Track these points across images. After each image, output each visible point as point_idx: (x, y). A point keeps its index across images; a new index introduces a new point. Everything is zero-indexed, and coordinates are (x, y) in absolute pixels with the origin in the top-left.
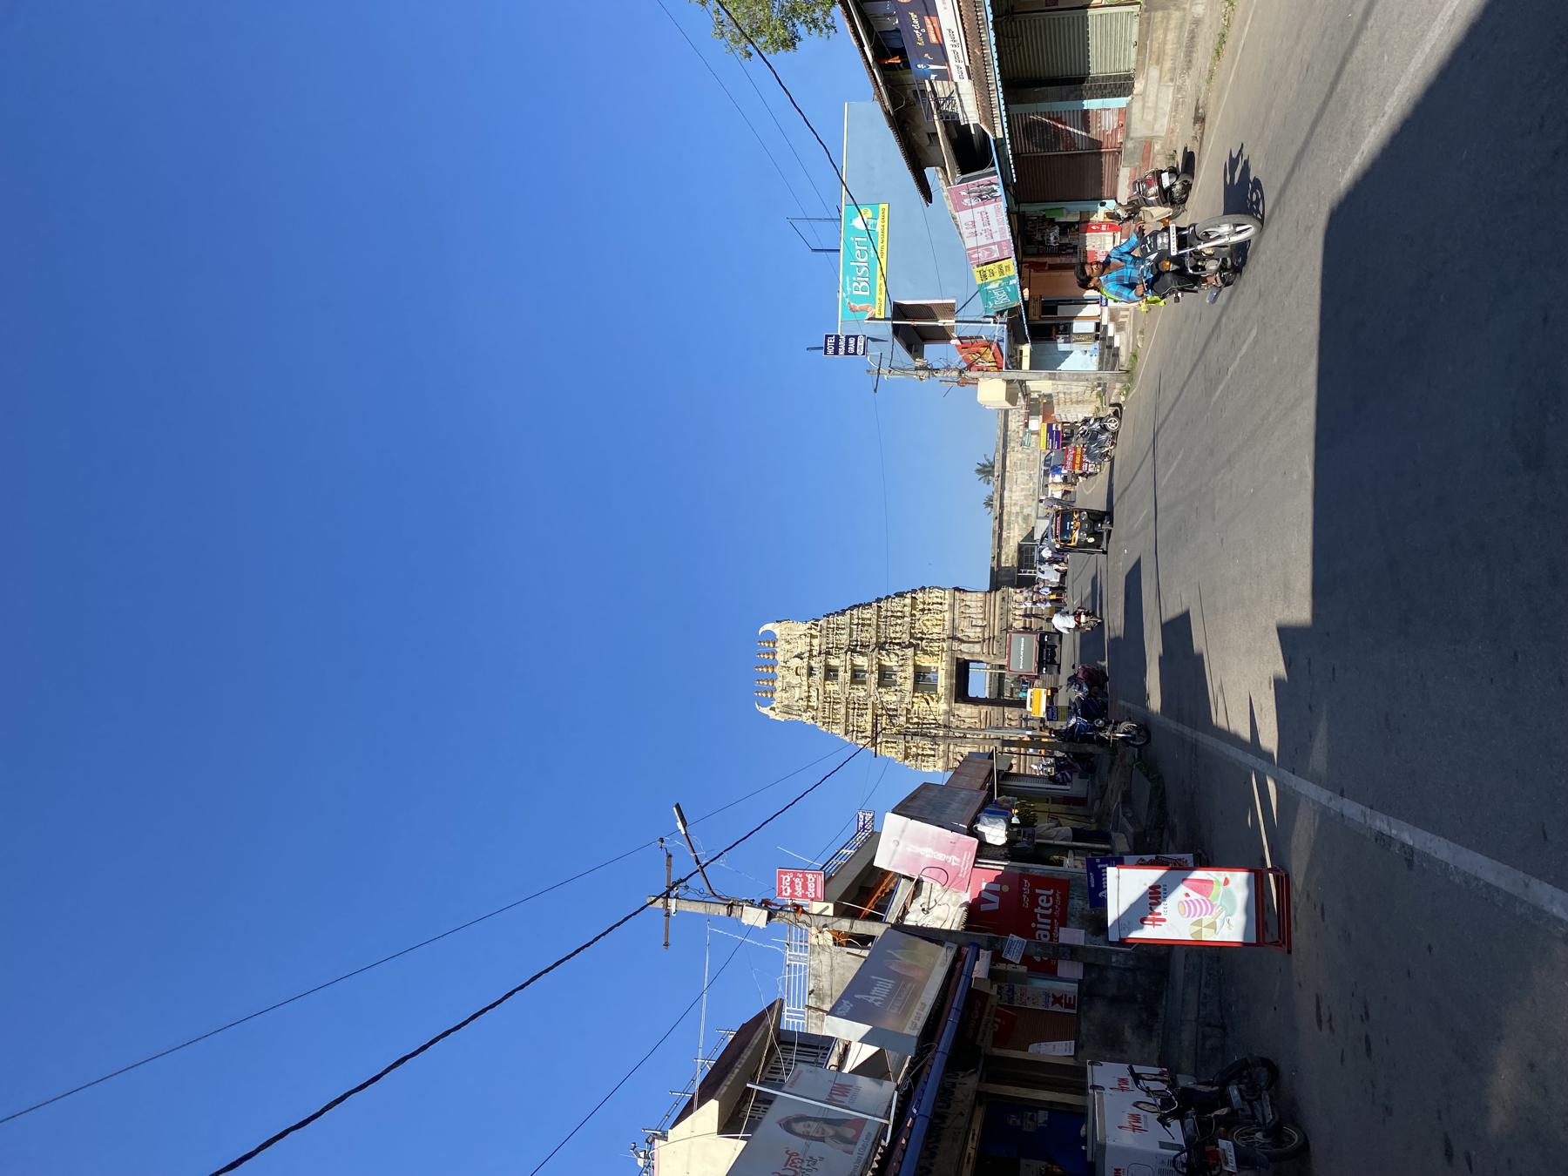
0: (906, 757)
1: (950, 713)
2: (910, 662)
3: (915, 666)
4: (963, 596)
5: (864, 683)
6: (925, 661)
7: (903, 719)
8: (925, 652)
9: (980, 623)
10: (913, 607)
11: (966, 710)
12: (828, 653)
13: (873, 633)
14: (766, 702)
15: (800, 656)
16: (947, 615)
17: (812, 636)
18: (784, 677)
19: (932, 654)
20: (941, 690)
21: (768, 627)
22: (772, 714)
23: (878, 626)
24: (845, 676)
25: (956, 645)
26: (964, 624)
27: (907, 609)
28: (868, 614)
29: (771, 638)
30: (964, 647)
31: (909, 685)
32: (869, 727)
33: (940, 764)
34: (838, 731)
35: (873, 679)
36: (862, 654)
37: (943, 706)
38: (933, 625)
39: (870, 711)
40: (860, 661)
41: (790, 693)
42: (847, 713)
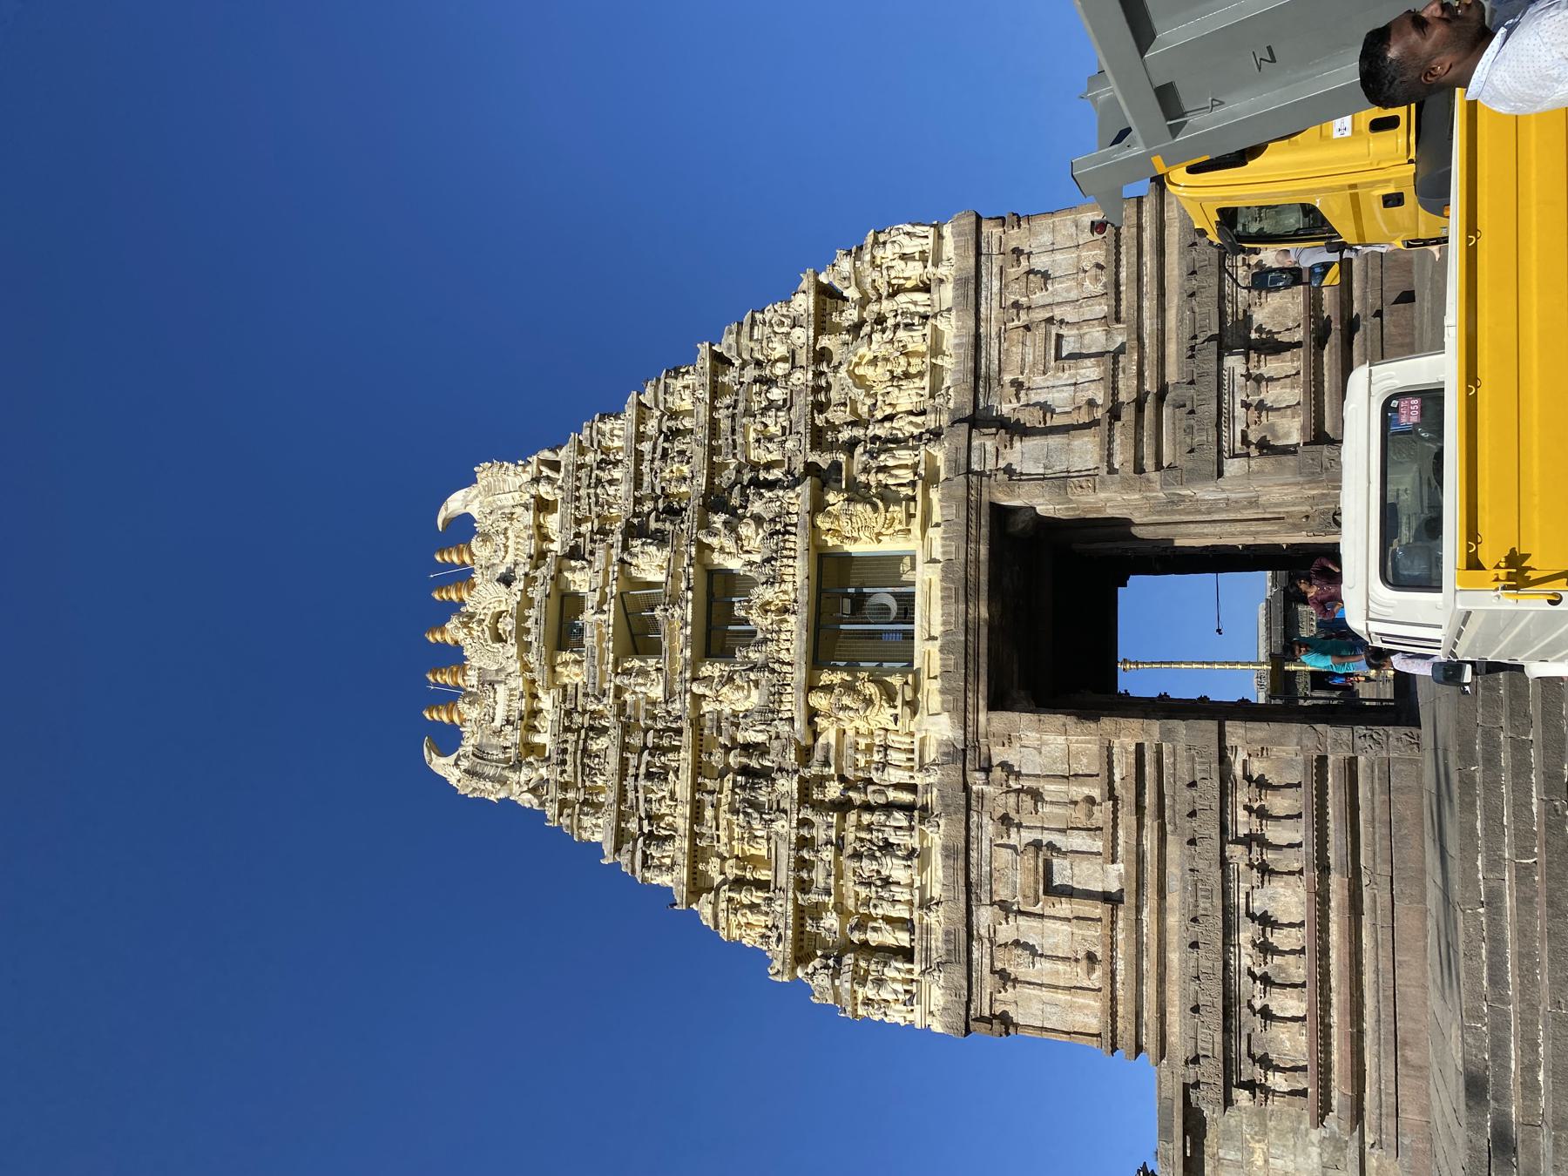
0: (801, 956)
1: (968, 755)
2: (798, 542)
3: (832, 569)
4: (1015, 237)
5: (654, 649)
6: (863, 535)
7: (787, 786)
8: (857, 493)
9: (1096, 338)
10: (822, 325)
11: (1043, 744)
12: (574, 553)
13: (699, 454)
14: (448, 740)
15: (506, 580)
16: (952, 329)
17: (543, 506)
18: (482, 656)
19: (887, 496)
20: (928, 654)
21: (456, 503)
22: (453, 776)
23: (713, 425)
24: (598, 622)
25: (986, 443)
26: (1019, 356)
27: (801, 336)
28: (686, 394)
29: (464, 528)
30: (1024, 455)
31: (792, 639)
32: (682, 825)
33: (936, 994)
34: (598, 830)
35: (679, 624)
36: (660, 539)
37: (937, 727)
38: (892, 381)
39: (686, 755)
40: (651, 565)
41: (499, 716)
42: (624, 762)
